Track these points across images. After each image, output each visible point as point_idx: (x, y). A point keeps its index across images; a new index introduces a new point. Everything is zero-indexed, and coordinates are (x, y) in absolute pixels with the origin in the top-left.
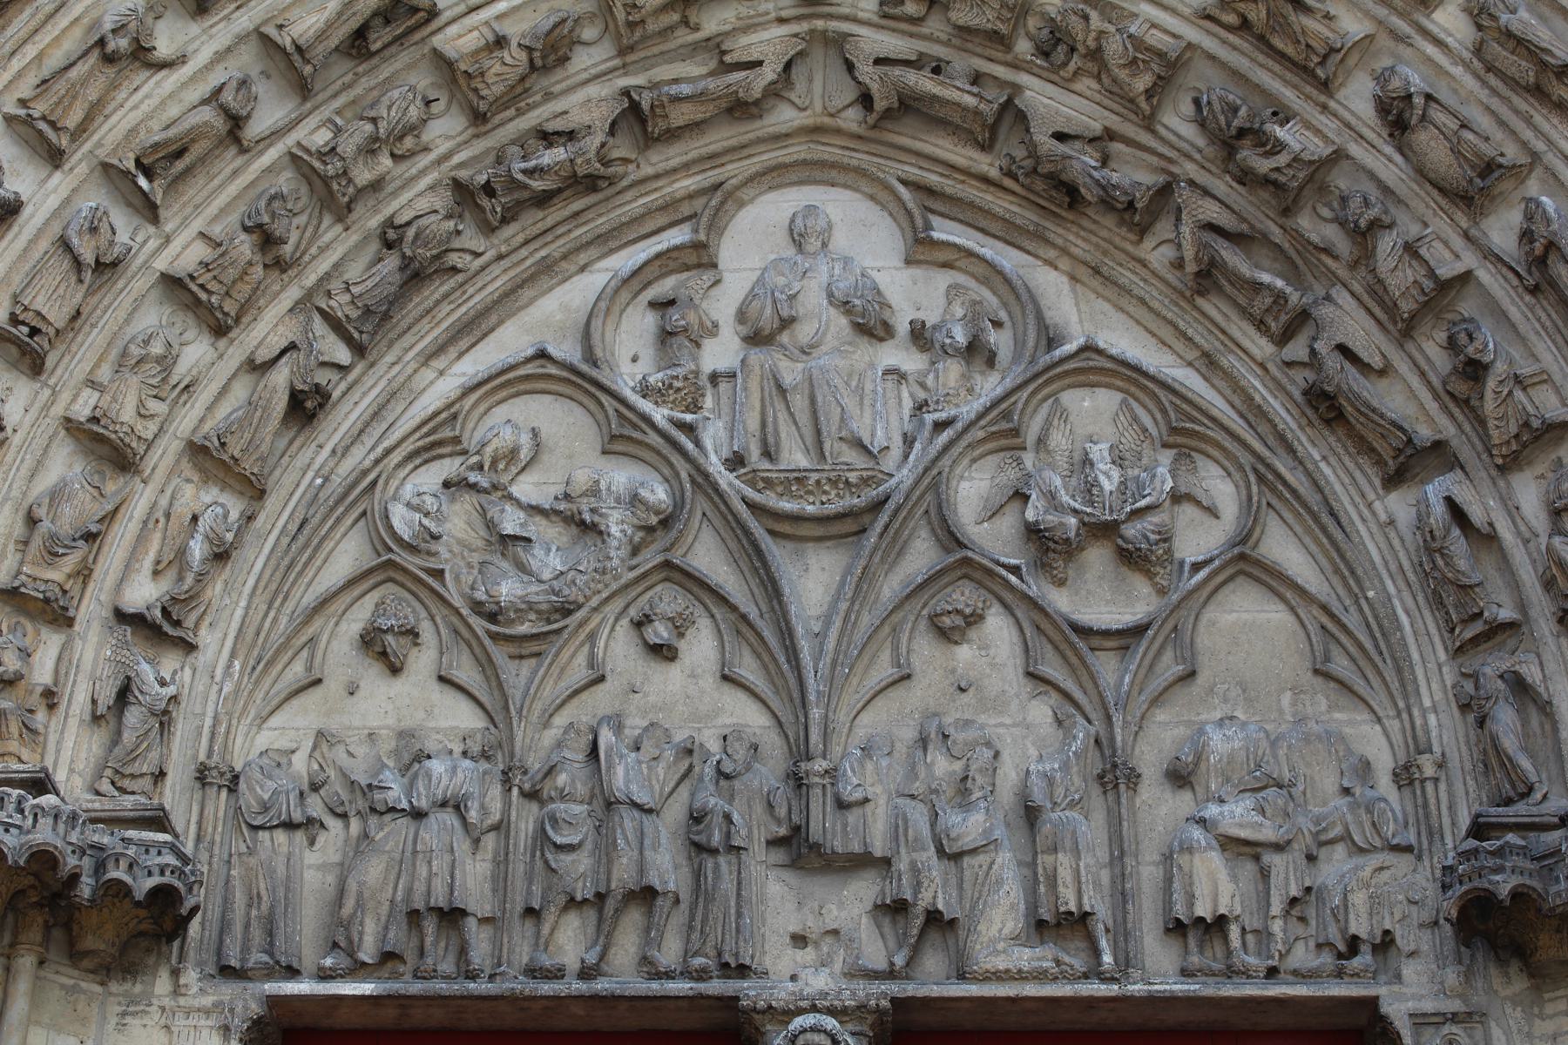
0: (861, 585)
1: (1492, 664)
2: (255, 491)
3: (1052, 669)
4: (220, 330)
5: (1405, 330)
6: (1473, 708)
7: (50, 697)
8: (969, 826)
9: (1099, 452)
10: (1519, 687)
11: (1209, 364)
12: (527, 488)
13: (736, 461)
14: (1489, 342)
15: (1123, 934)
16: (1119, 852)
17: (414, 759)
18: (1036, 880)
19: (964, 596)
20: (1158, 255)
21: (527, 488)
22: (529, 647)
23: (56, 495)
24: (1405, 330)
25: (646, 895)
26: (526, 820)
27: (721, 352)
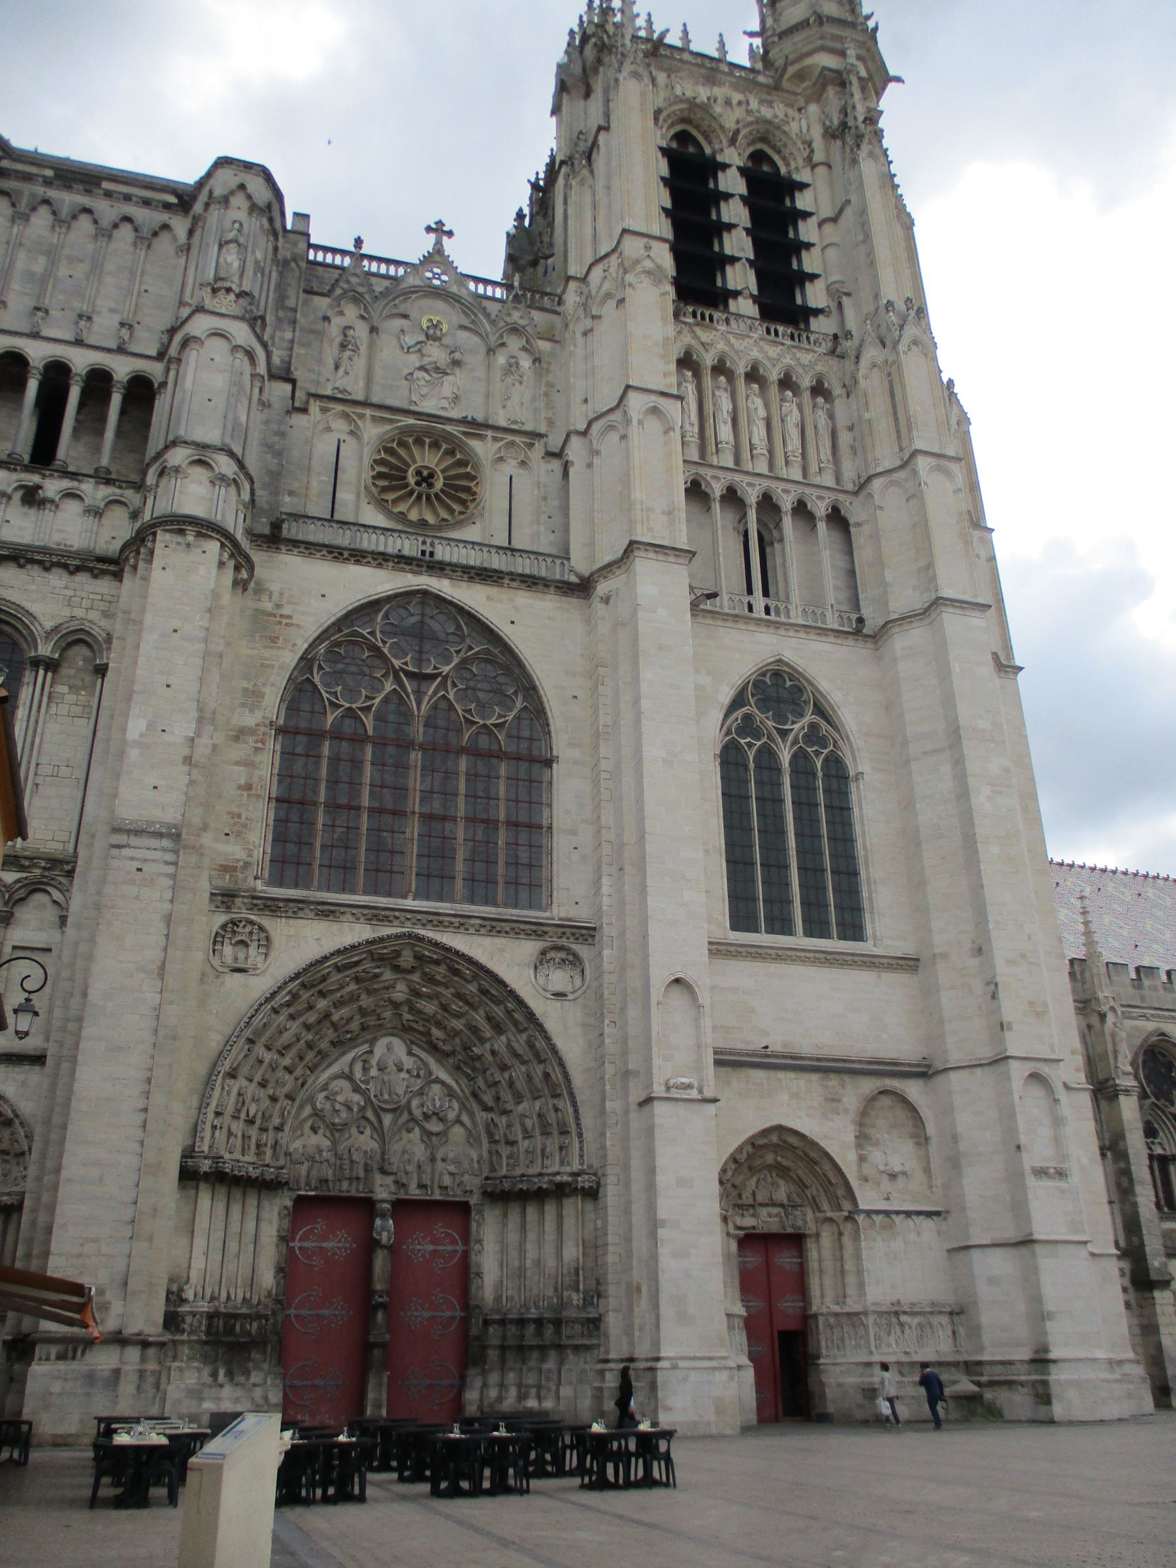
0: (394, 1122)
1: (494, 1147)
2: (293, 1100)
3: (425, 1139)
4: (291, 1072)
5: (489, 1087)
6: (490, 1152)
7: (266, 1145)
8: (410, 1168)
9: (437, 1098)
10: (497, 1152)
11: (457, 1082)
12: (339, 1098)
13: (376, 1096)
14: (502, 1093)
15: (432, 1189)
16: (433, 1173)
17: (320, 1151)
18: (419, 1179)
19: (411, 1125)
20: (451, 1060)
21: (339, 1098)
22: (338, 1130)
23: (267, 1108)
24: (489, 1087)
25: (358, 1179)
26: (338, 1163)
27: (374, 1072)
